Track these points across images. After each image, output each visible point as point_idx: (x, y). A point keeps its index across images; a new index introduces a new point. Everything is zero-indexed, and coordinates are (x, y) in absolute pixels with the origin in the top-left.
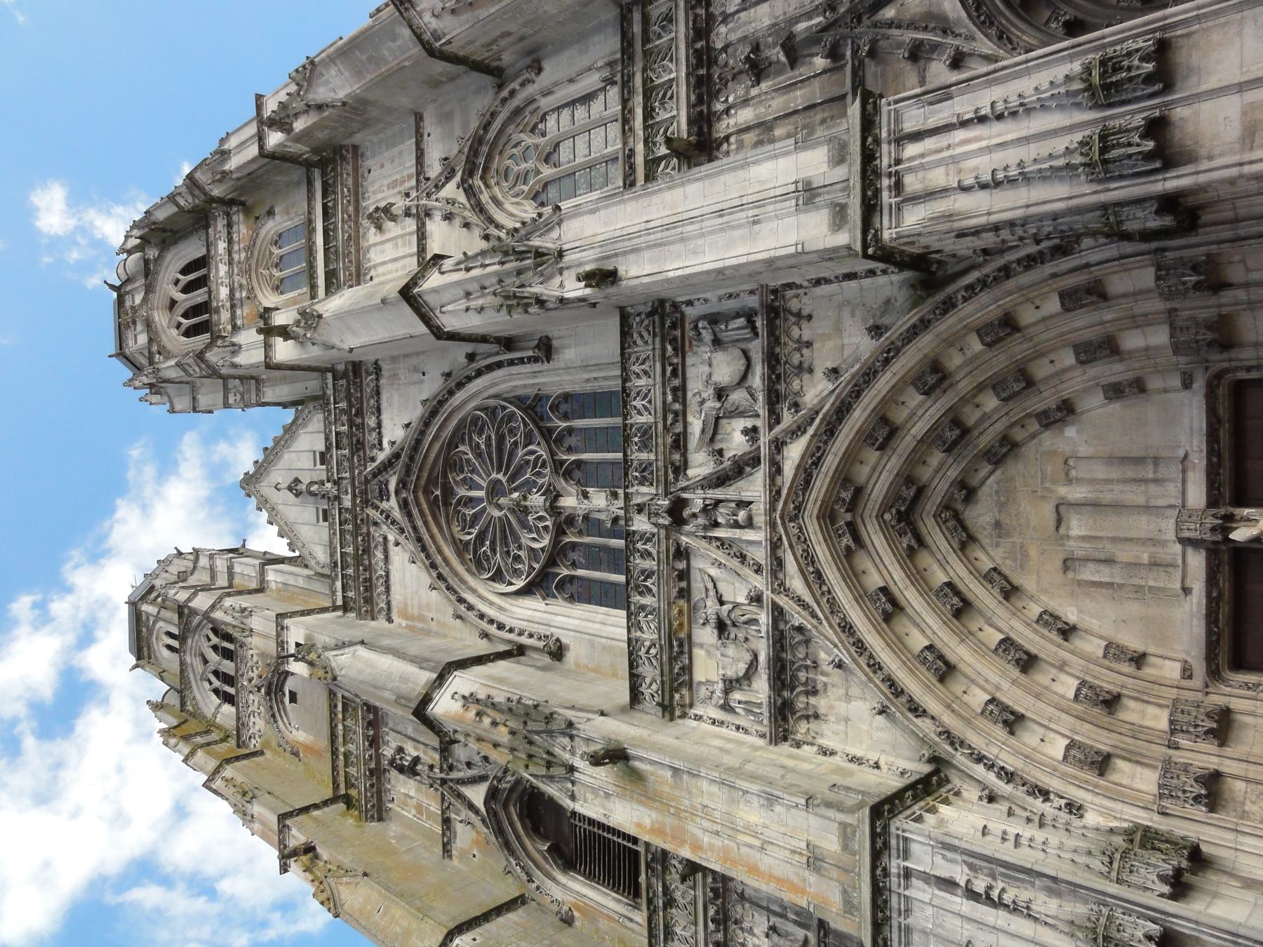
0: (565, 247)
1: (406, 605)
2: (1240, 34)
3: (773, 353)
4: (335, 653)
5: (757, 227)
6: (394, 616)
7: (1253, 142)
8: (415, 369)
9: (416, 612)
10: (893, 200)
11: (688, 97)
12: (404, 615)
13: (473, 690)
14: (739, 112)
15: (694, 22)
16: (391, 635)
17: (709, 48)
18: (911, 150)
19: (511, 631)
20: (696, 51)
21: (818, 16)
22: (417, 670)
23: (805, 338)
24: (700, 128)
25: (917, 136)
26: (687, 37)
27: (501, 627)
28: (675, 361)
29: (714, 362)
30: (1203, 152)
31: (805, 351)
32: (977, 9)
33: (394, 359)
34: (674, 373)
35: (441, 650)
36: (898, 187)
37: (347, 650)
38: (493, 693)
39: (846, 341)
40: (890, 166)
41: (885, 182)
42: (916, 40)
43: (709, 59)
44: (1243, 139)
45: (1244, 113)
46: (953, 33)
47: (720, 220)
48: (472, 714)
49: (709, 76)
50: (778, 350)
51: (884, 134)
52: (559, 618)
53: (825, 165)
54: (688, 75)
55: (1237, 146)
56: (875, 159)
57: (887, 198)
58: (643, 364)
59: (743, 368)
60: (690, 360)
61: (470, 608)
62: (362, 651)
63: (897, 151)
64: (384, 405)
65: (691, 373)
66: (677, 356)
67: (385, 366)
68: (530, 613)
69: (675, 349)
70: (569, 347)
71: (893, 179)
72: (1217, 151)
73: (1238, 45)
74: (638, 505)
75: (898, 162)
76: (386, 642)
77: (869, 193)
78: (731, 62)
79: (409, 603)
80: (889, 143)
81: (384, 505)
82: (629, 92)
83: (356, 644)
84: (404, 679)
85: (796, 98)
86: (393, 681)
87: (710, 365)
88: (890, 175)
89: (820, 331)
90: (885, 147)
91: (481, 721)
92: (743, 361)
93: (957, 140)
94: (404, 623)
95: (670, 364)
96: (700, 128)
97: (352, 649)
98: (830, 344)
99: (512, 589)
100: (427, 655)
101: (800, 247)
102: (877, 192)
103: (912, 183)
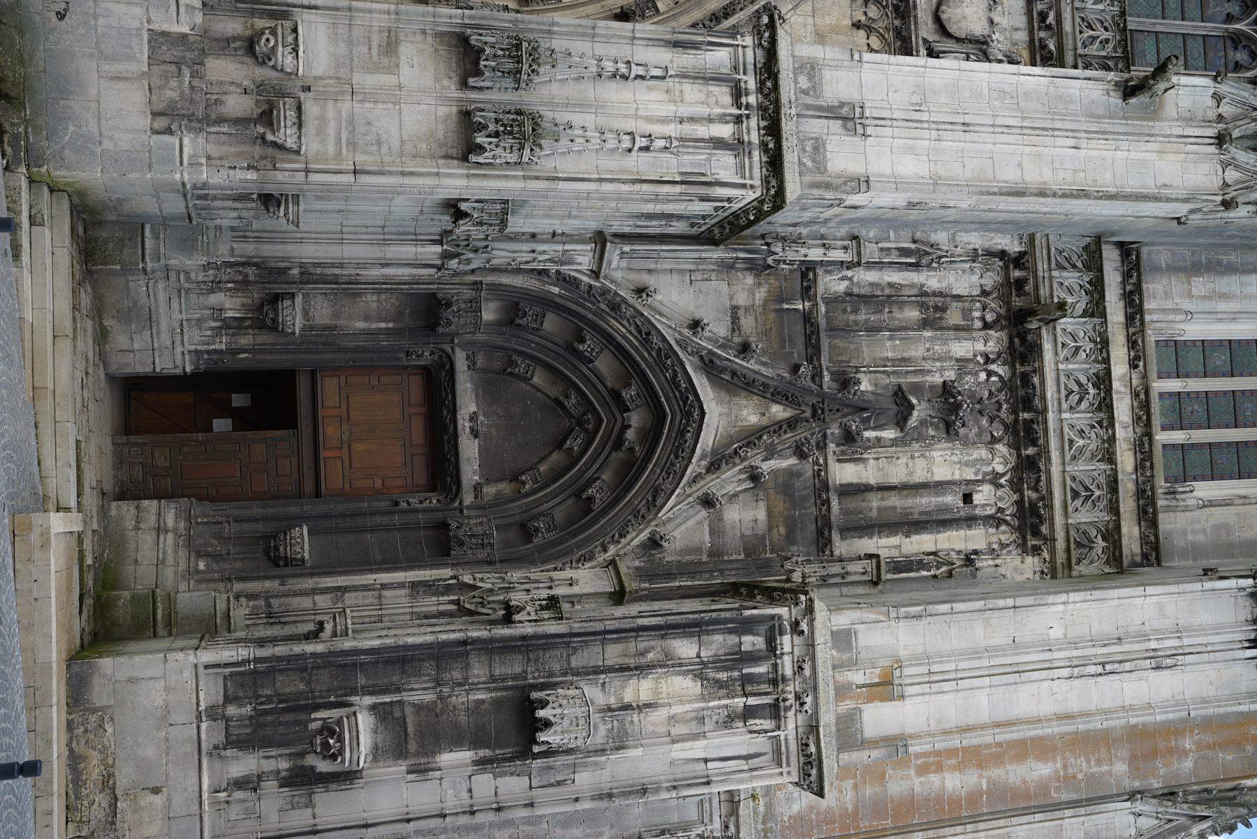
0: (1213, 149)
2: (402, 142)
3: (903, 18)
5: (916, 99)
7: (389, 36)
10: (741, 76)
11: (1043, 382)
14: (970, 355)
15: (1038, 480)
17: (1016, 446)
18: (725, 131)
20: (1034, 442)
21: (868, 440)
23: (862, 33)
24: (1023, 340)
25: (718, 143)
26: (1049, 459)
28: (1043, 34)
29: (986, 24)
30: (429, 39)
31: (863, 19)
32: (675, 373)
34: (1043, 16)
36: (738, 93)
39: (810, 20)
40: (748, 117)
41: (752, 99)
42: (743, 359)
43: (1015, 433)
44: (397, 42)
45: (397, 66)
46: (701, 358)
47: (968, 119)
49: (1015, 412)
50: (897, 23)
51: (756, 153)
53: (829, 147)
54: (1045, 410)
55: (402, 37)
56: (765, 128)
57: (751, 82)
58: (1094, 38)
59: (943, 8)
60: (1022, 36)
63: (740, 132)
65: (1021, 21)
66: (1040, 40)
69: (1044, 47)
71: (744, 100)
72: (419, 37)
73: (404, 132)
75: (738, 120)
77: (769, 84)
78: (984, 422)
80: (750, 143)
82: (1142, 444)
85: (894, 349)
87: (991, 22)
88: (748, 107)
89: (843, 38)
90: (755, 138)
92: (944, 17)
93: (672, 126)
95: (1049, 27)
96: (1023, 340)
98: (828, 20)
101: (856, 57)
102: (760, 90)
103: (723, 95)
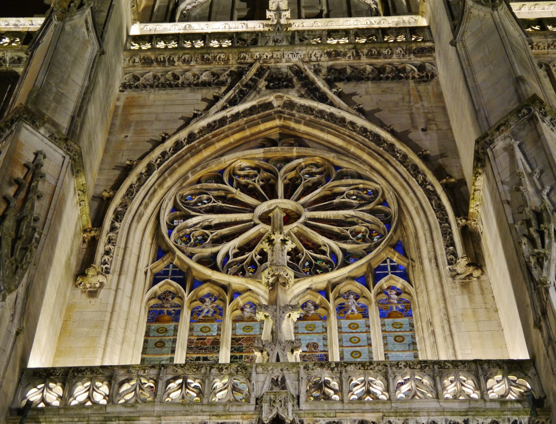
1: (142, 106)
4: (90, 20)
6: (128, 93)
8: (428, 121)
9: (134, 118)
12: (129, 105)
13: (48, 177)
16: (108, 86)
19: (113, 229)
22: (70, 112)
27: (118, 216)
33: (440, 96)
35: (90, 144)
37: (93, 34)
38: (45, 202)
48: (19, 174)
52: (129, 286)
61: (141, 180)
62: (91, 50)
64: (385, 85)
67: (430, 87)
68: (135, 251)
70: (471, 300)
74: (283, 380)
76: (101, 80)
79: (145, 110)
81: (262, 84)
83: (100, 46)
84: (59, 98)
86: (57, 86)
91: (10, 184)
94: (120, 104)
97: (94, 40)
99: (164, 230)
100: (88, 126)
